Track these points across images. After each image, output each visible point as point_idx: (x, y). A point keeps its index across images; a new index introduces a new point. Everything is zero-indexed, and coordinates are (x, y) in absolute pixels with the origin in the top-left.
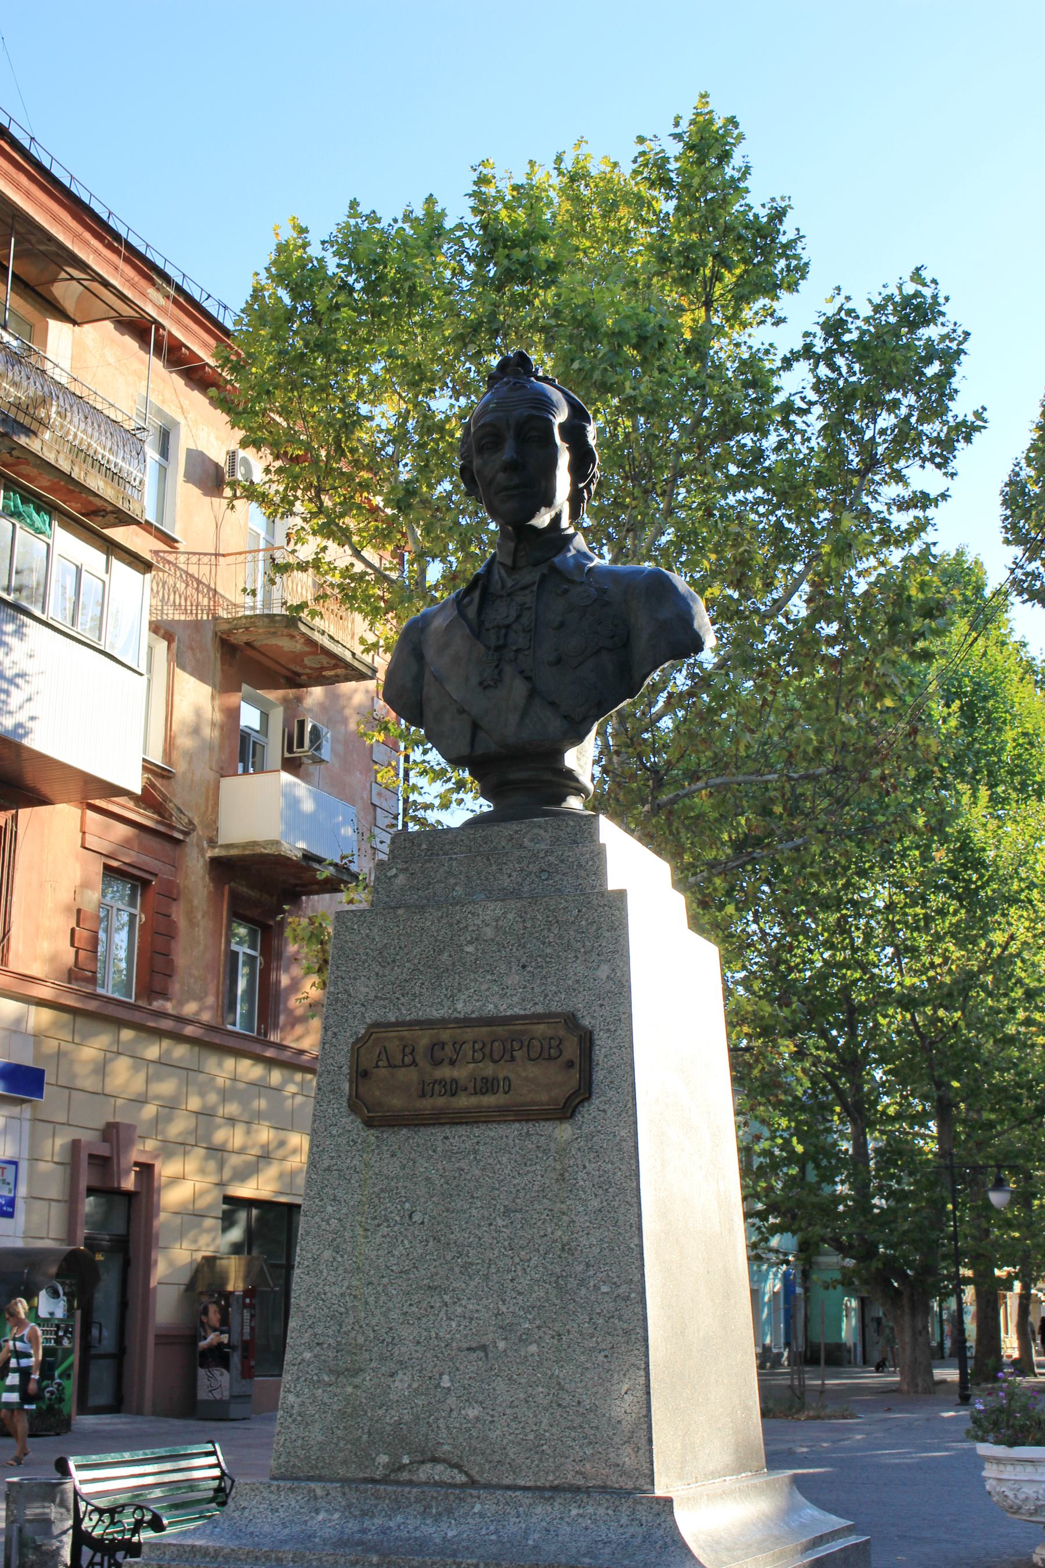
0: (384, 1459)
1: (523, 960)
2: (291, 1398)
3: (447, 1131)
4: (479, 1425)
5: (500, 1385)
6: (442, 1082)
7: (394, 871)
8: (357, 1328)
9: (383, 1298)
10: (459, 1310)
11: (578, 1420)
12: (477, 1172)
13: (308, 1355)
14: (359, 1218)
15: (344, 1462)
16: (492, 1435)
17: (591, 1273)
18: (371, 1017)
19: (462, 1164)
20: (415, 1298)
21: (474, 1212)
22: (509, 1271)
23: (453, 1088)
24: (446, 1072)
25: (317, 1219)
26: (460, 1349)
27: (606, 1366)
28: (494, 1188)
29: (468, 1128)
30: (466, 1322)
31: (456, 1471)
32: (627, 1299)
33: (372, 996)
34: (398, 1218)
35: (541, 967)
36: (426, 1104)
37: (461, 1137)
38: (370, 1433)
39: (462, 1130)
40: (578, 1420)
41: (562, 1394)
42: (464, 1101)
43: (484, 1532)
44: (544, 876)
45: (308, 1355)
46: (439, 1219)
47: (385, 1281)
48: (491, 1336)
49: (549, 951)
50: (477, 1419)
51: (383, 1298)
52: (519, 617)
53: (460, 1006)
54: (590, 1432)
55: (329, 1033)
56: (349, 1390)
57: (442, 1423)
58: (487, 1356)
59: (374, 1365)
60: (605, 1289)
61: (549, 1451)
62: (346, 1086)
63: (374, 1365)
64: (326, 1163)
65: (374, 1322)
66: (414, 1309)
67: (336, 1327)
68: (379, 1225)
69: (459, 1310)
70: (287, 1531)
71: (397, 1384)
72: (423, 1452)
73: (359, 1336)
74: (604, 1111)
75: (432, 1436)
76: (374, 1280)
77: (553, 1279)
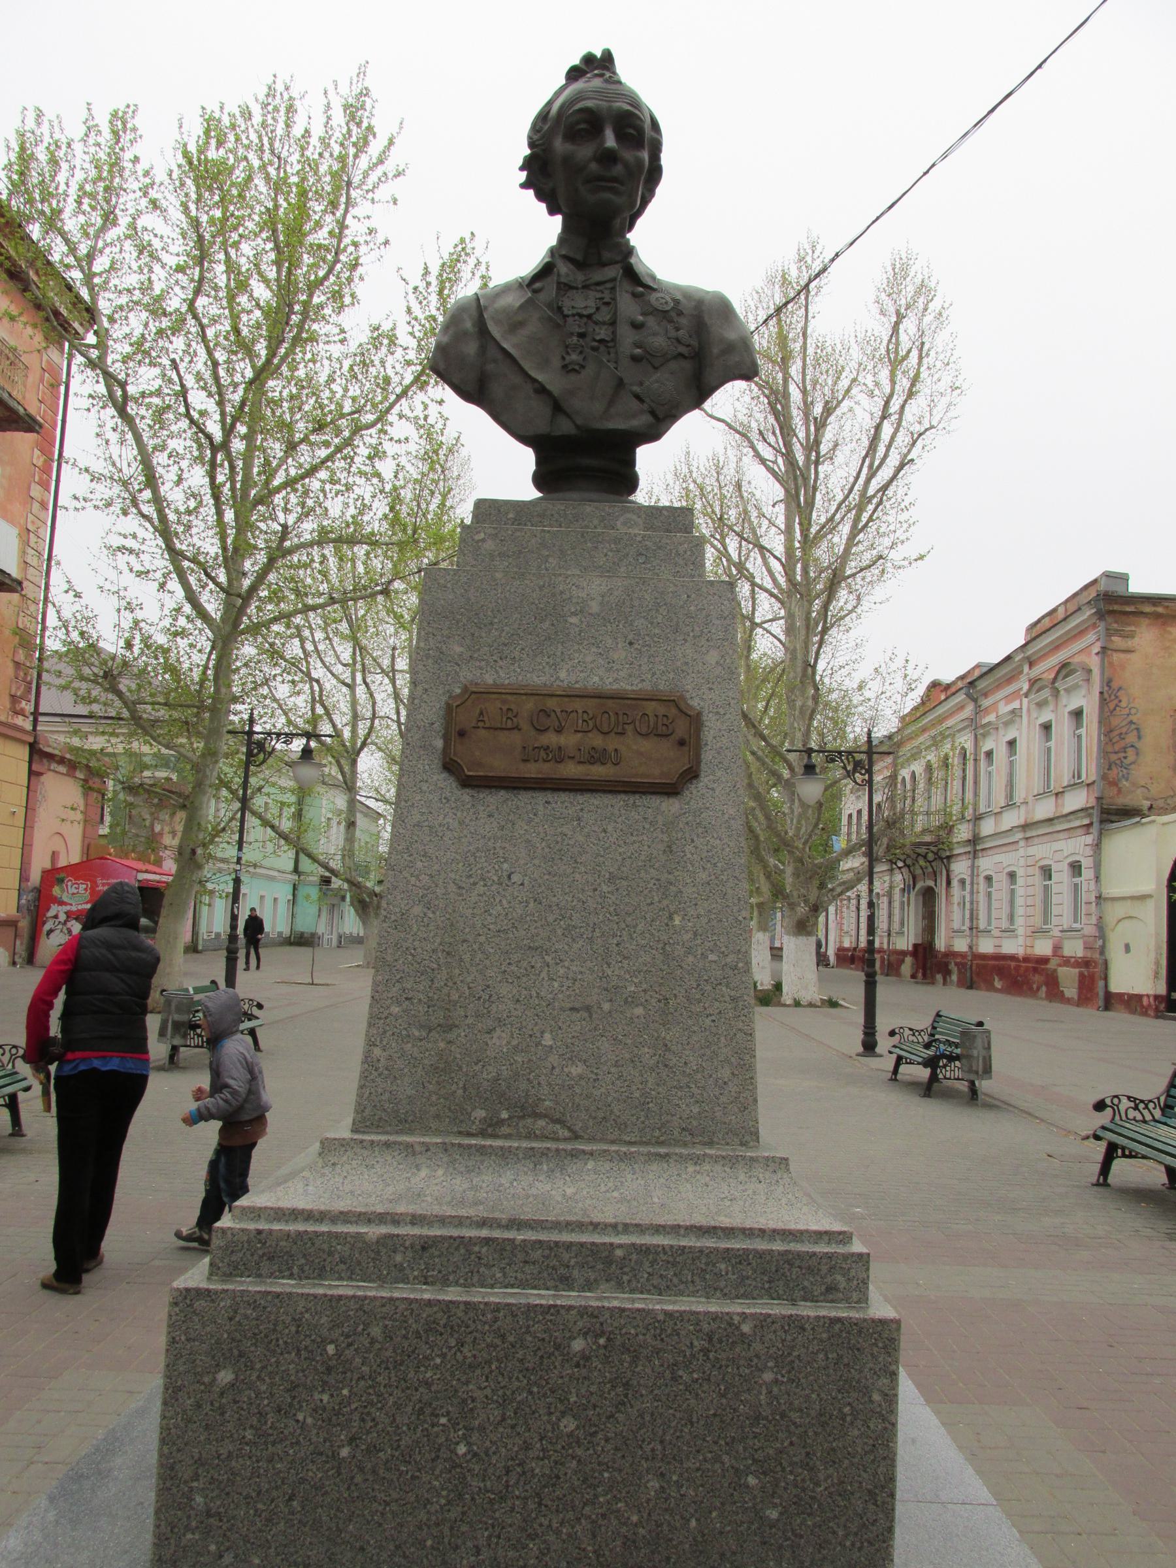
0: (480, 1113)
1: (630, 637)
3: (549, 796)
4: (583, 1083)
6: (547, 749)
8: (450, 984)
9: (480, 956)
10: (562, 971)
11: (686, 1080)
12: (581, 839)
13: (395, 1010)
14: (453, 875)
15: (437, 1116)
16: (597, 1093)
17: (699, 942)
18: (467, 674)
19: (565, 829)
20: (515, 957)
21: (577, 876)
22: (614, 936)
23: (559, 756)
24: (551, 739)
26: (562, 1009)
27: (714, 1030)
28: (598, 855)
29: (572, 795)
30: (569, 983)
31: (558, 1126)
34: (495, 878)
35: (649, 646)
36: (532, 770)
37: (564, 803)
38: (465, 1089)
39: (564, 796)
40: (686, 1080)
41: (669, 1055)
42: (571, 770)
43: (603, 1188)
45: (395, 1010)
46: (540, 881)
47: (482, 939)
48: (595, 998)
49: (657, 631)
50: (581, 1077)
51: (480, 956)
52: (598, 309)
53: (563, 675)
54: (695, 1090)
55: (419, 688)
56: (442, 1045)
58: (591, 1017)
59: (470, 1021)
60: (712, 957)
61: (655, 1109)
62: (439, 743)
63: (470, 1021)
64: (417, 817)
65: (469, 979)
66: (513, 968)
68: (475, 884)
69: (562, 971)
70: (391, 1189)
71: (494, 1041)
72: (523, 1108)
73: (453, 992)
74: (713, 789)
75: (533, 1092)
76: (470, 938)
77: (660, 946)
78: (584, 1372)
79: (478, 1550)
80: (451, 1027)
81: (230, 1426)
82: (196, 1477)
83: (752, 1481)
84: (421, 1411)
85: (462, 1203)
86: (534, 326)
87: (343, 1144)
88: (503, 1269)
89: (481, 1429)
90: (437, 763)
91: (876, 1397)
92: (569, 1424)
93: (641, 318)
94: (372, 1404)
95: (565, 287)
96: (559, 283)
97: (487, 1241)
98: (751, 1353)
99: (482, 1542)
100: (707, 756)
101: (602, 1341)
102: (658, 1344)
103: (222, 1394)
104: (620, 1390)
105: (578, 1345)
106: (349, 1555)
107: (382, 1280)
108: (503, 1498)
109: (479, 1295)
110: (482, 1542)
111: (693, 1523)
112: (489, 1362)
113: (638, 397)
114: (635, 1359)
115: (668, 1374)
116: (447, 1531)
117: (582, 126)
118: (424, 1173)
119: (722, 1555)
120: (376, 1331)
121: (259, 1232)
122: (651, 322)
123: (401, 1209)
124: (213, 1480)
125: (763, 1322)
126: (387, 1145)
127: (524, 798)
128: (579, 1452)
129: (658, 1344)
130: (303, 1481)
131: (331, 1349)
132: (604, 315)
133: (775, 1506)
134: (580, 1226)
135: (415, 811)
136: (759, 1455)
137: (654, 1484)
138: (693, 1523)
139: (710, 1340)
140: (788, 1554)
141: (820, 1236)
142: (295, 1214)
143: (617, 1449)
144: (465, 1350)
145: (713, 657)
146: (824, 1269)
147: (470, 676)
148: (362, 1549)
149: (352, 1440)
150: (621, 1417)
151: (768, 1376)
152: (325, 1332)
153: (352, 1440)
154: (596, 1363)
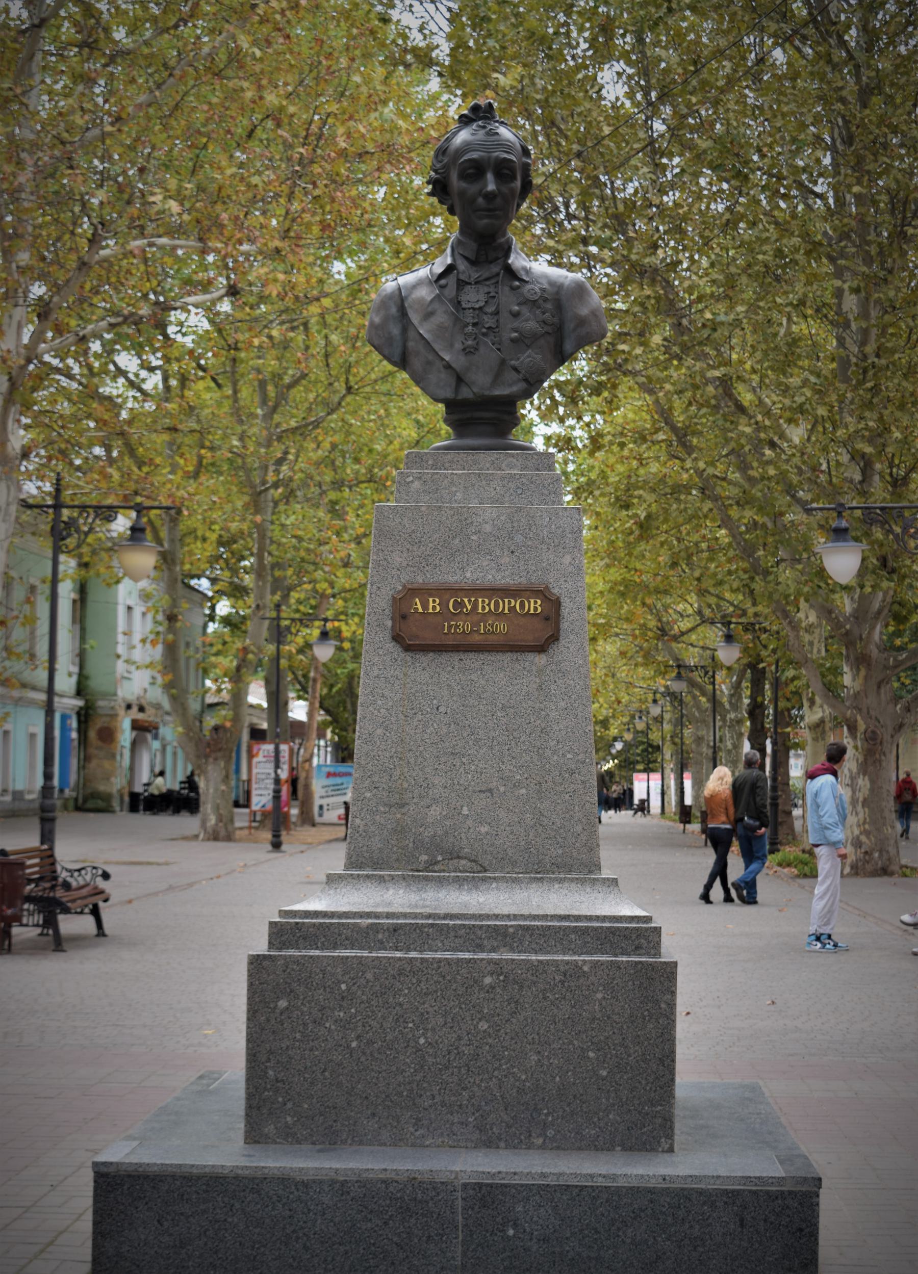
0: (424, 858)
2: (358, 821)
3: (462, 655)
5: (502, 813)
7: (411, 478)
9: (420, 759)
12: (483, 682)
13: (368, 795)
18: (405, 577)
19: (472, 677)
25: (371, 708)
26: (474, 792)
32: (584, 762)
33: (404, 564)
39: (472, 655)
44: (519, 491)
45: (368, 795)
47: (421, 748)
50: (487, 833)
51: (420, 759)
53: (468, 575)
54: (560, 840)
56: (399, 816)
57: (463, 835)
59: (415, 800)
60: (569, 756)
62: (389, 623)
63: (415, 800)
64: (376, 672)
67: (388, 777)
72: (451, 854)
78: (492, 996)
79: (433, 1097)
80: (403, 806)
81: (287, 1031)
82: (269, 1060)
83: (591, 1054)
84: (397, 1020)
85: (416, 906)
86: (441, 318)
87: (340, 876)
88: (442, 941)
89: (433, 1029)
90: (388, 635)
91: (663, 1006)
92: (483, 1026)
93: (516, 308)
94: (369, 1017)
95: (461, 284)
96: (458, 280)
97: (432, 925)
98: (589, 983)
99: (436, 1092)
100: (564, 625)
101: (501, 978)
102: (534, 978)
103: (281, 1014)
104: (513, 1005)
105: (488, 980)
106: (359, 1102)
107: (371, 950)
108: (447, 1068)
109: (428, 955)
110: (436, 1092)
111: (558, 1079)
112: (436, 992)
113: (516, 369)
114: (521, 987)
115: (541, 996)
116: (414, 1086)
117: (471, 171)
118: (391, 892)
119: (575, 1096)
120: (369, 976)
121: (297, 923)
122: (525, 310)
123: (380, 910)
124: (278, 1062)
125: (595, 965)
126: (368, 876)
127: (444, 657)
128: (490, 1041)
129: (534, 978)
130: (331, 1061)
131: (343, 987)
132: (491, 309)
133: (605, 1068)
134: (488, 917)
135: (375, 668)
136: (595, 1040)
137: (535, 1057)
138: (558, 1079)
139: (565, 975)
140: (613, 1095)
141: (632, 919)
142: (316, 914)
143: (512, 1039)
144: (422, 985)
145: (567, 559)
146: (634, 936)
147: (407, 578)
148: (366, 1098)
149: (358, 1037)
150: (514, 1020)
151: (599, 996)
152: (340, 977)
153: (358, 1037)
154: (498, 990)
